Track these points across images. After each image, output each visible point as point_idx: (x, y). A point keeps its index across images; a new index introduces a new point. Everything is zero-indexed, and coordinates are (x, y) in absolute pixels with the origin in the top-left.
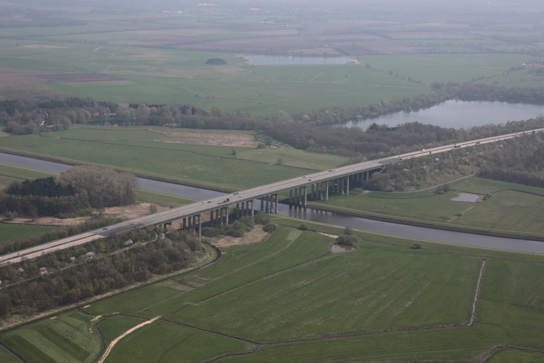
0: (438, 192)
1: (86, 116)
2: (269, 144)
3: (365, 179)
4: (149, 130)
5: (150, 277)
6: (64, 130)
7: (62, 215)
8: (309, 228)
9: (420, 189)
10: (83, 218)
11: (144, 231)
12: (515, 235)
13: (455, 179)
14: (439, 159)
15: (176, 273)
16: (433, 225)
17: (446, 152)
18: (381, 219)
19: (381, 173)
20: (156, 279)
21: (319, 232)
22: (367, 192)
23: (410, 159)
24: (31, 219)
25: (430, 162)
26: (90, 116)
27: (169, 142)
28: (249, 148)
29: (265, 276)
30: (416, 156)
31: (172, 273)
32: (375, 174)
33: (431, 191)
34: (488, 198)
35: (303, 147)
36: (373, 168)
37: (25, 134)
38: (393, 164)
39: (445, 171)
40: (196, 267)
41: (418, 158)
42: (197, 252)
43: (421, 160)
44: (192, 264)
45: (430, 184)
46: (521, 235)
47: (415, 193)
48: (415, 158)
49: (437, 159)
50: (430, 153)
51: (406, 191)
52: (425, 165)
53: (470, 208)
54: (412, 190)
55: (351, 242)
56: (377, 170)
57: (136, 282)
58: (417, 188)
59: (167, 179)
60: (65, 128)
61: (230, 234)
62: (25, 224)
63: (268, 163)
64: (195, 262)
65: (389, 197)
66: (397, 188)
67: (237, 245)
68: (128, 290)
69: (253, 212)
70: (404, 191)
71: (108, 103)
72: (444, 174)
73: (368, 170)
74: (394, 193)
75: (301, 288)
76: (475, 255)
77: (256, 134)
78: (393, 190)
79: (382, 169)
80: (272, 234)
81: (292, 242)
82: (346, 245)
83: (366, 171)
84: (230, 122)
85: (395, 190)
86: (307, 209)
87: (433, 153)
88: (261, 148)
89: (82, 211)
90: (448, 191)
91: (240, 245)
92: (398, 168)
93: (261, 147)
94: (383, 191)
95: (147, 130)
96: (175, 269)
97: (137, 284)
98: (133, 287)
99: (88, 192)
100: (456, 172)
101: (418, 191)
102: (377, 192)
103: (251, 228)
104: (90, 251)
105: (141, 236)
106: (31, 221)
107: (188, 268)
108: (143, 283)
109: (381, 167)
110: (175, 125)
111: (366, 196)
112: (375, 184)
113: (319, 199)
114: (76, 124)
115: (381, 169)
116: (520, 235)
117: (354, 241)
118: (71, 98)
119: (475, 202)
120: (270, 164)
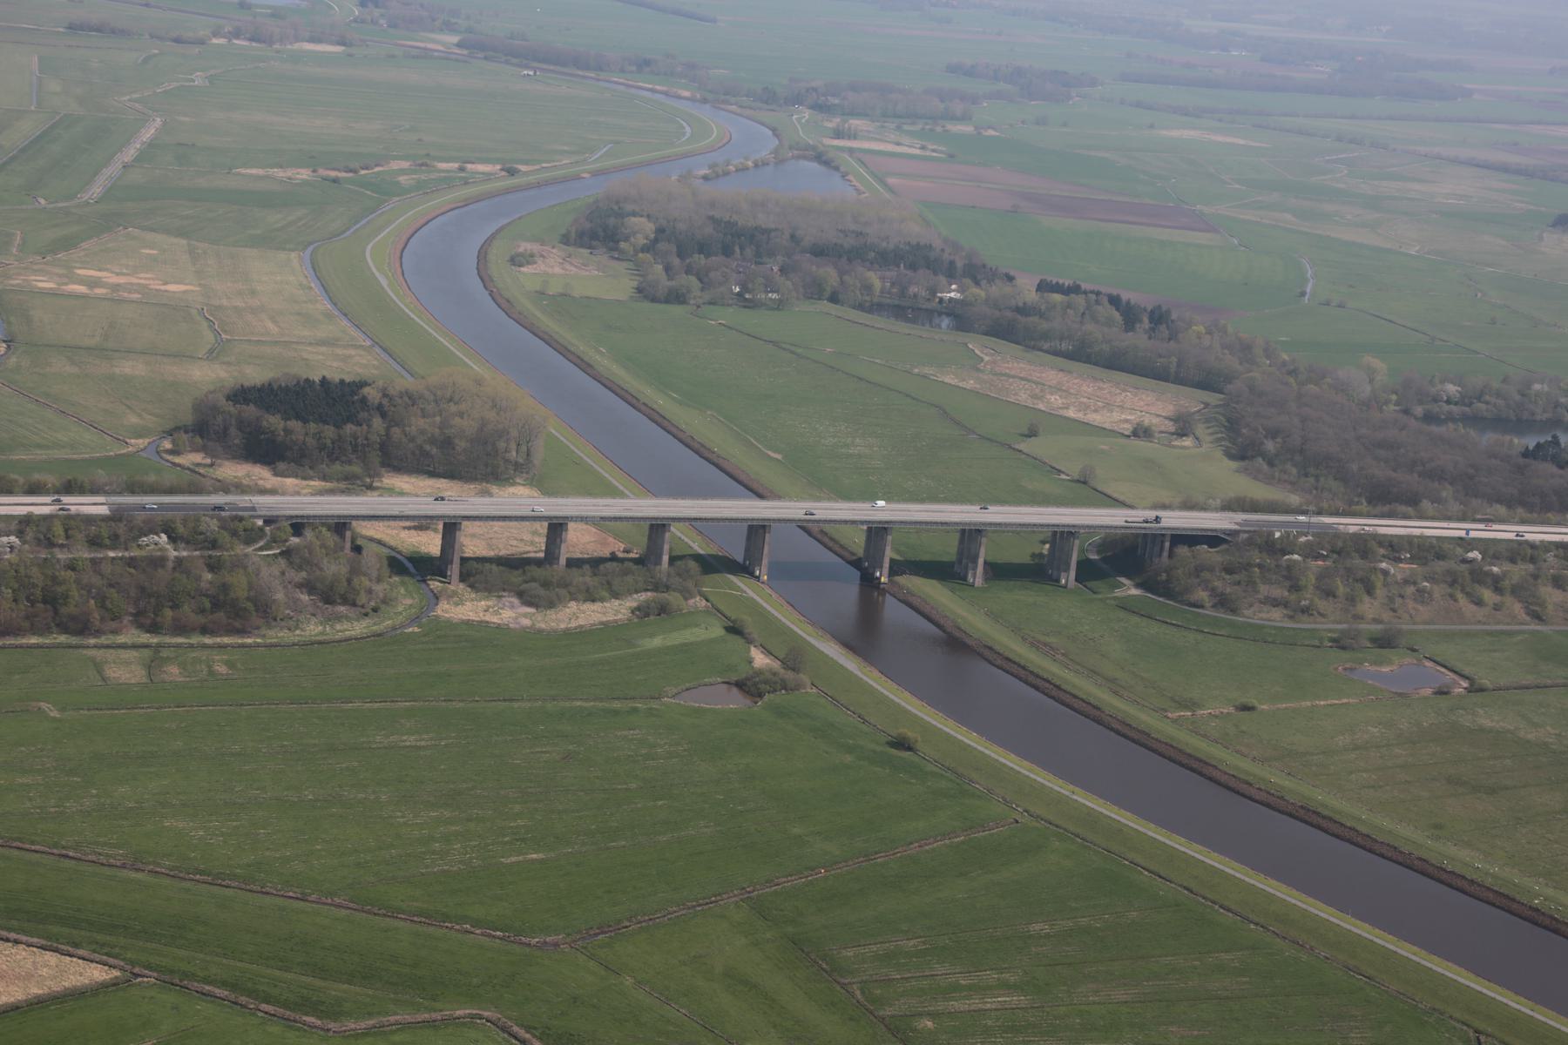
0: (1340, 643)
1: (868, 288)
2: (1181, 434)
3: (1160, 555)
4: (970, 346)
5: (115, 632)
6: (773, 309)
7: (282, 466)
8: (746, 631)
9: (1297, 622)
10: (323, 484)
11: (214, 525)
12: (1268, 793)
13: (1484, 624)
14: (1480, 557)
15: (195, 639)
16: (1098, 708)
17: (1538, 543)
18: (999, 662)
19: (1216, 552)
20: (119, 641)
21: (755, 646)
22: (1134, 592)
23: (1354, 534)
24: (208, 461)
25: (1440, 556)
26: (878, 290)
27: (953, 382)
28: (1113, 431)
29: (369, 700)
30: (1382, 531)
31: (187, 638)
32: (1183, 551)
33: (1329, 635)
34: (1470, 692)
35: (1243, 452)
36: (1184, 529)
37: (667, 301)
38: (1277, 535)
39: (1468, 594)
40: (269, 641)
41: (1392, 536)
42: (342, 608)
43: (1394, 547)
44: (271, 633)
45: (1358, 618)
46: (1286, 798)
47: (1263, 627)
48: (1375, 536)
49: (1475, 555)
50: (1467, 534)
51: (1245, 617)
52: (1412, 560)
53: (1337, 702)
54: (1276, 616)
55: (763, 687)
56: (1213, 539)
57: (58, 633)
58: (1291, 617)
59: (714, 453)
60: (779, 305)
61: (520, 595)
62: (189, 469)
63: (1060, 472)
64: (290, 630)
65: (1169, 621)
66: (1223, 602)
67: (487, 622)
68: (10, 644)
69: (666, 558)
70: (1238, 615)
71: (991, 269)
72: (1456, 600)
73: (1169, 532)
74: (1199, 613)
75: (373, 749)
76: (1014, 806)
77: (1217, 406)
78: (1207, 605)
79: (1231, 542)
80: (636, 620)
81: (639, 649)
82: (747, 693)
83: (1163, 535)
84: (1174, 359)
85: (1213, 606)
86: (887, 595)
87: (1473, 534)
88: (1139, 437)
89: (337, 467)
90: (1393, 648)
91: (494, 623)
92: (1278, 546)
93: (1141, 434)
94: (1176, 602)
95: (966, 344)
96: (204, 631)
97: (55, 638)
98: (34, 640)
99: (388, 429)
100: (1518, 608)
101: (1295, 626)
102: (1161, 599)
103: (605, 594)
104: (20, 534)
105: (201, 533)
106: (205, 466)
107: (249, 637)
108: (74, 640)
109: (1228, 535)
110: (1046, 346)
111: (1113, 602)
112: (1164, 577)
113: (965, 578)
114: (825, 302)
115: (1223, 541)
116: (1282, 798)
117: (779, 687)
118: (918, 244)
119: (1396, 693)
120: (1063, 477)
